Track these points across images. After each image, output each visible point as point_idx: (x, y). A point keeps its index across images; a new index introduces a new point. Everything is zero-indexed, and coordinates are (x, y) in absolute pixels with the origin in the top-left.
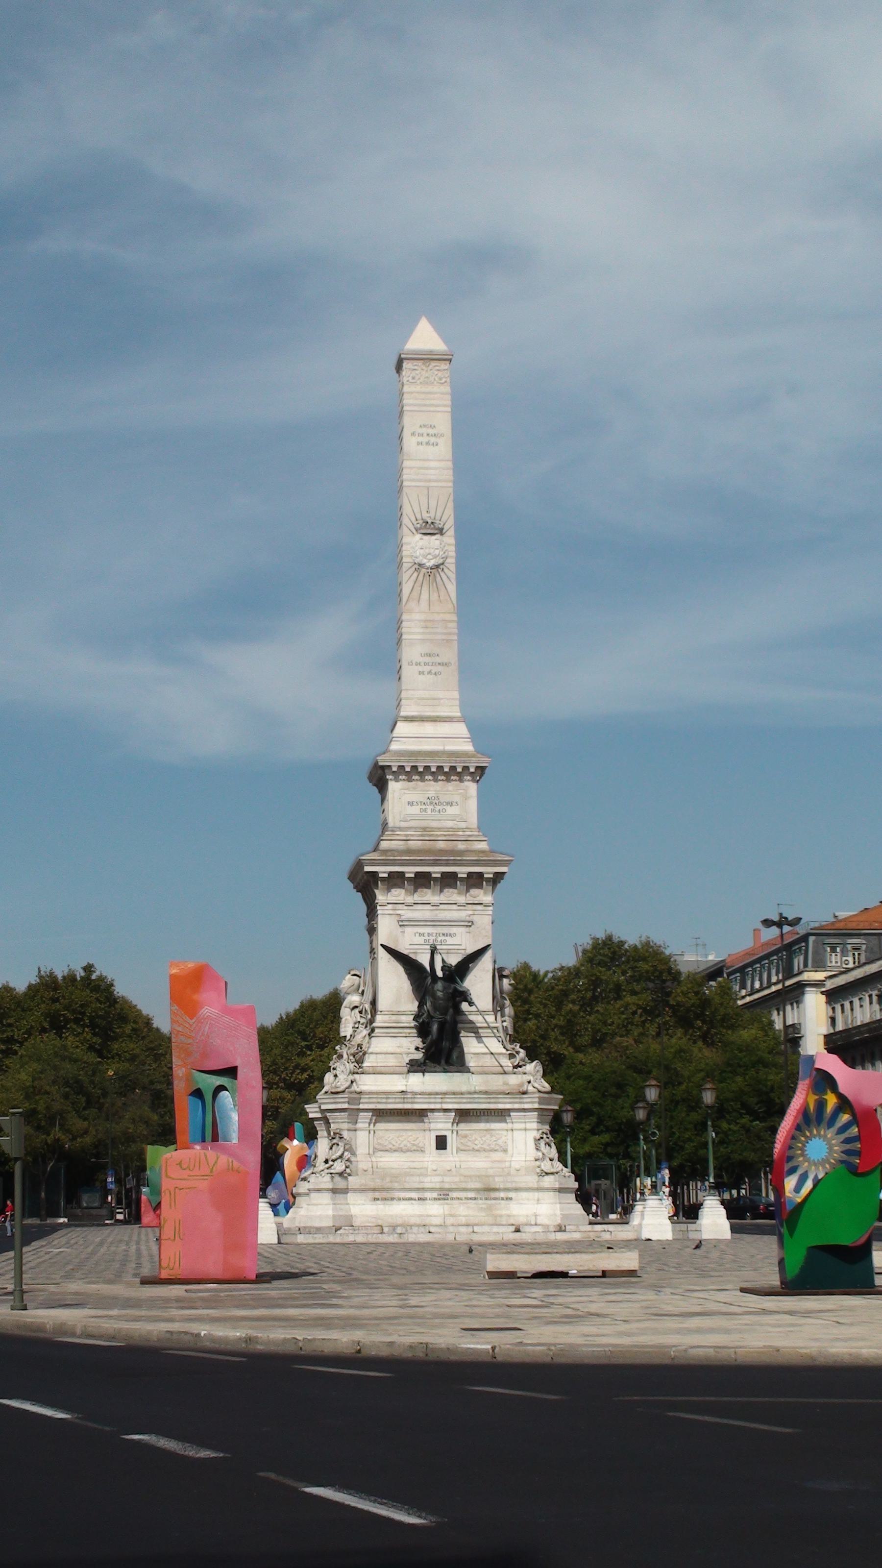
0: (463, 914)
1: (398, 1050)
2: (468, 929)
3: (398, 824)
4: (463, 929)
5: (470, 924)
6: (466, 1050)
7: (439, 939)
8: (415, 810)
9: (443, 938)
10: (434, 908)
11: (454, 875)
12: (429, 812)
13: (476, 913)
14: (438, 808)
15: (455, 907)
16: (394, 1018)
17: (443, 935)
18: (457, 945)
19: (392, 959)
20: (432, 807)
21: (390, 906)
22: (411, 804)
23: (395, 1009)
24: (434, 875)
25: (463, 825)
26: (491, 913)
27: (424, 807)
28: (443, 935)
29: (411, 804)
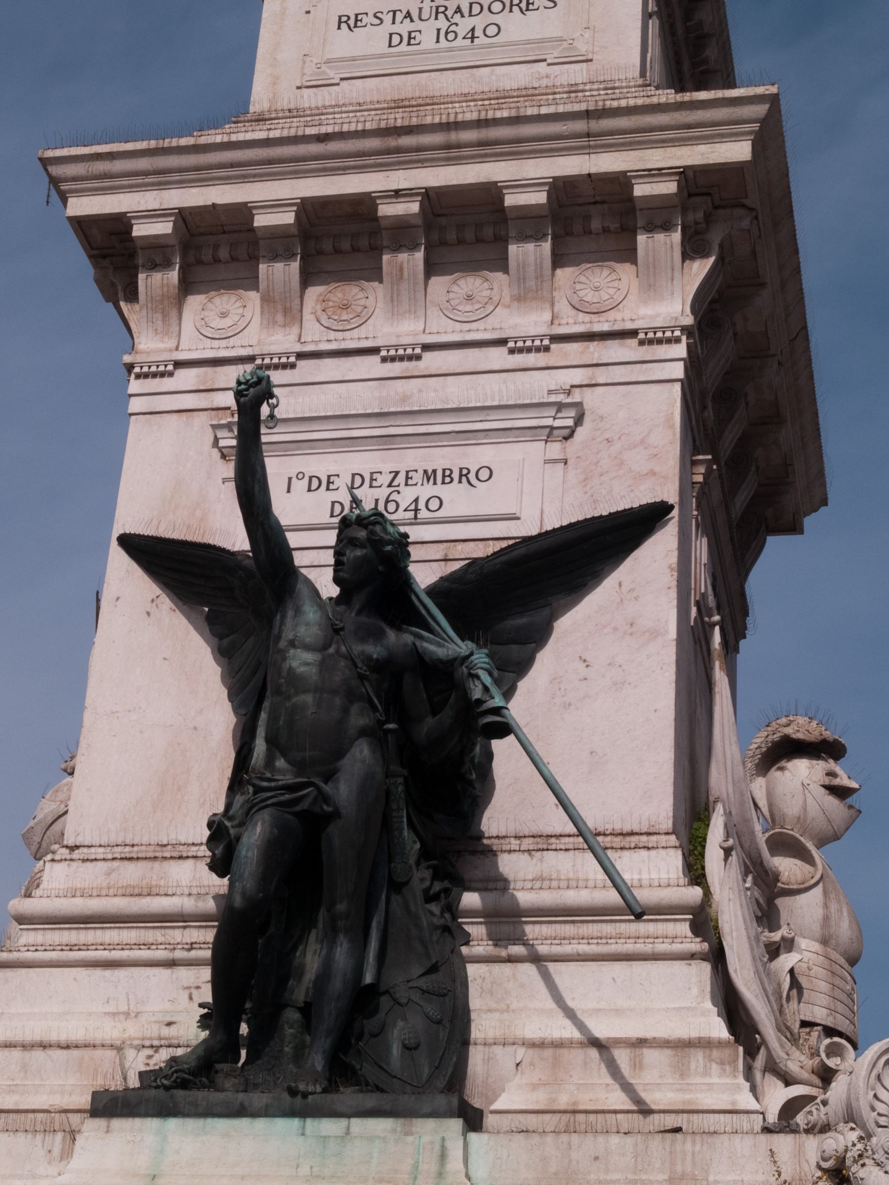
0: (537, 386)
1: (110, 1031)
2: (555, 449)
3: (287, 98)
4: (536, 450)
5: (563, 423)
6: (482, 1026)
7: (406, 497)
8: (370, 41)
9: (426, 491)
10: (397, 368)
11: (490, 195)
12: (427, 40)
13: (601, 376)
14: (464, 25)
15: (497, 357)
16: (131, 873)
17: (429, 476)
18: (479, 504)
19: (166, 602)
20: (442, 23)
21: (187, 378)
22: (350, 22)
23: (147, 834)
24: (386, 210)
25: (576, 74)
26: (678, 371)
27: (404, 28)
28: (429, 476)
29: (350, 22)
